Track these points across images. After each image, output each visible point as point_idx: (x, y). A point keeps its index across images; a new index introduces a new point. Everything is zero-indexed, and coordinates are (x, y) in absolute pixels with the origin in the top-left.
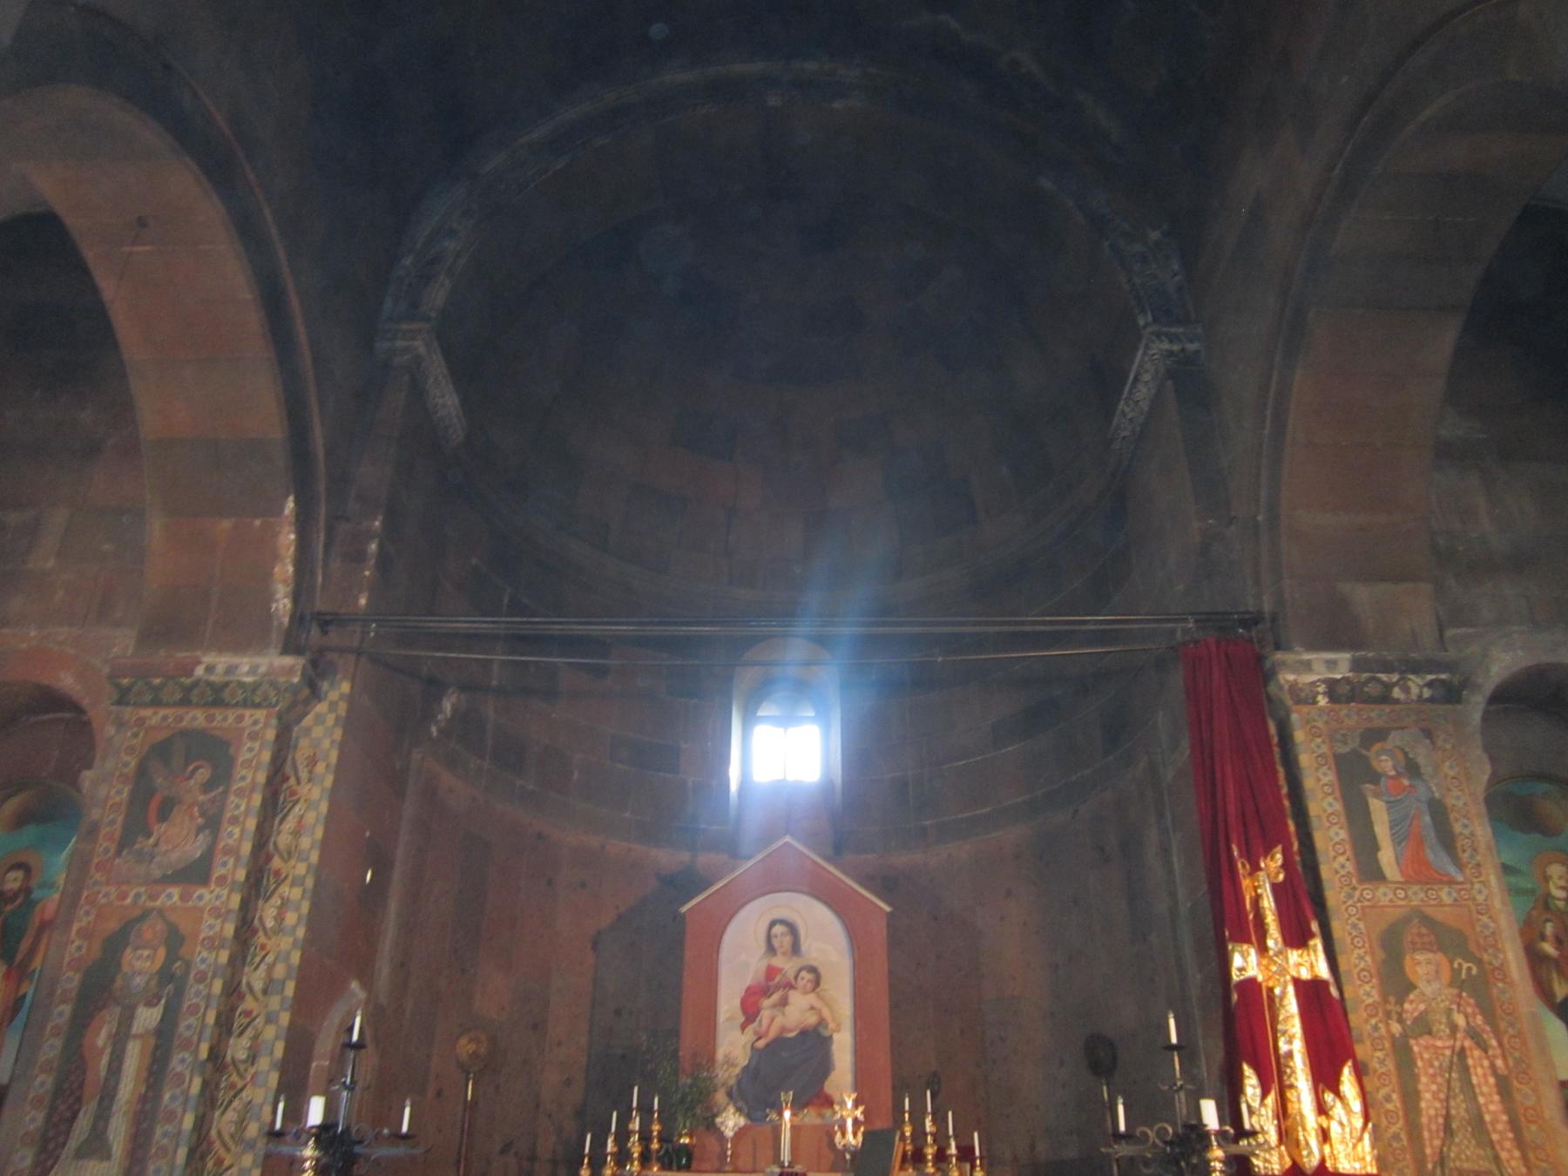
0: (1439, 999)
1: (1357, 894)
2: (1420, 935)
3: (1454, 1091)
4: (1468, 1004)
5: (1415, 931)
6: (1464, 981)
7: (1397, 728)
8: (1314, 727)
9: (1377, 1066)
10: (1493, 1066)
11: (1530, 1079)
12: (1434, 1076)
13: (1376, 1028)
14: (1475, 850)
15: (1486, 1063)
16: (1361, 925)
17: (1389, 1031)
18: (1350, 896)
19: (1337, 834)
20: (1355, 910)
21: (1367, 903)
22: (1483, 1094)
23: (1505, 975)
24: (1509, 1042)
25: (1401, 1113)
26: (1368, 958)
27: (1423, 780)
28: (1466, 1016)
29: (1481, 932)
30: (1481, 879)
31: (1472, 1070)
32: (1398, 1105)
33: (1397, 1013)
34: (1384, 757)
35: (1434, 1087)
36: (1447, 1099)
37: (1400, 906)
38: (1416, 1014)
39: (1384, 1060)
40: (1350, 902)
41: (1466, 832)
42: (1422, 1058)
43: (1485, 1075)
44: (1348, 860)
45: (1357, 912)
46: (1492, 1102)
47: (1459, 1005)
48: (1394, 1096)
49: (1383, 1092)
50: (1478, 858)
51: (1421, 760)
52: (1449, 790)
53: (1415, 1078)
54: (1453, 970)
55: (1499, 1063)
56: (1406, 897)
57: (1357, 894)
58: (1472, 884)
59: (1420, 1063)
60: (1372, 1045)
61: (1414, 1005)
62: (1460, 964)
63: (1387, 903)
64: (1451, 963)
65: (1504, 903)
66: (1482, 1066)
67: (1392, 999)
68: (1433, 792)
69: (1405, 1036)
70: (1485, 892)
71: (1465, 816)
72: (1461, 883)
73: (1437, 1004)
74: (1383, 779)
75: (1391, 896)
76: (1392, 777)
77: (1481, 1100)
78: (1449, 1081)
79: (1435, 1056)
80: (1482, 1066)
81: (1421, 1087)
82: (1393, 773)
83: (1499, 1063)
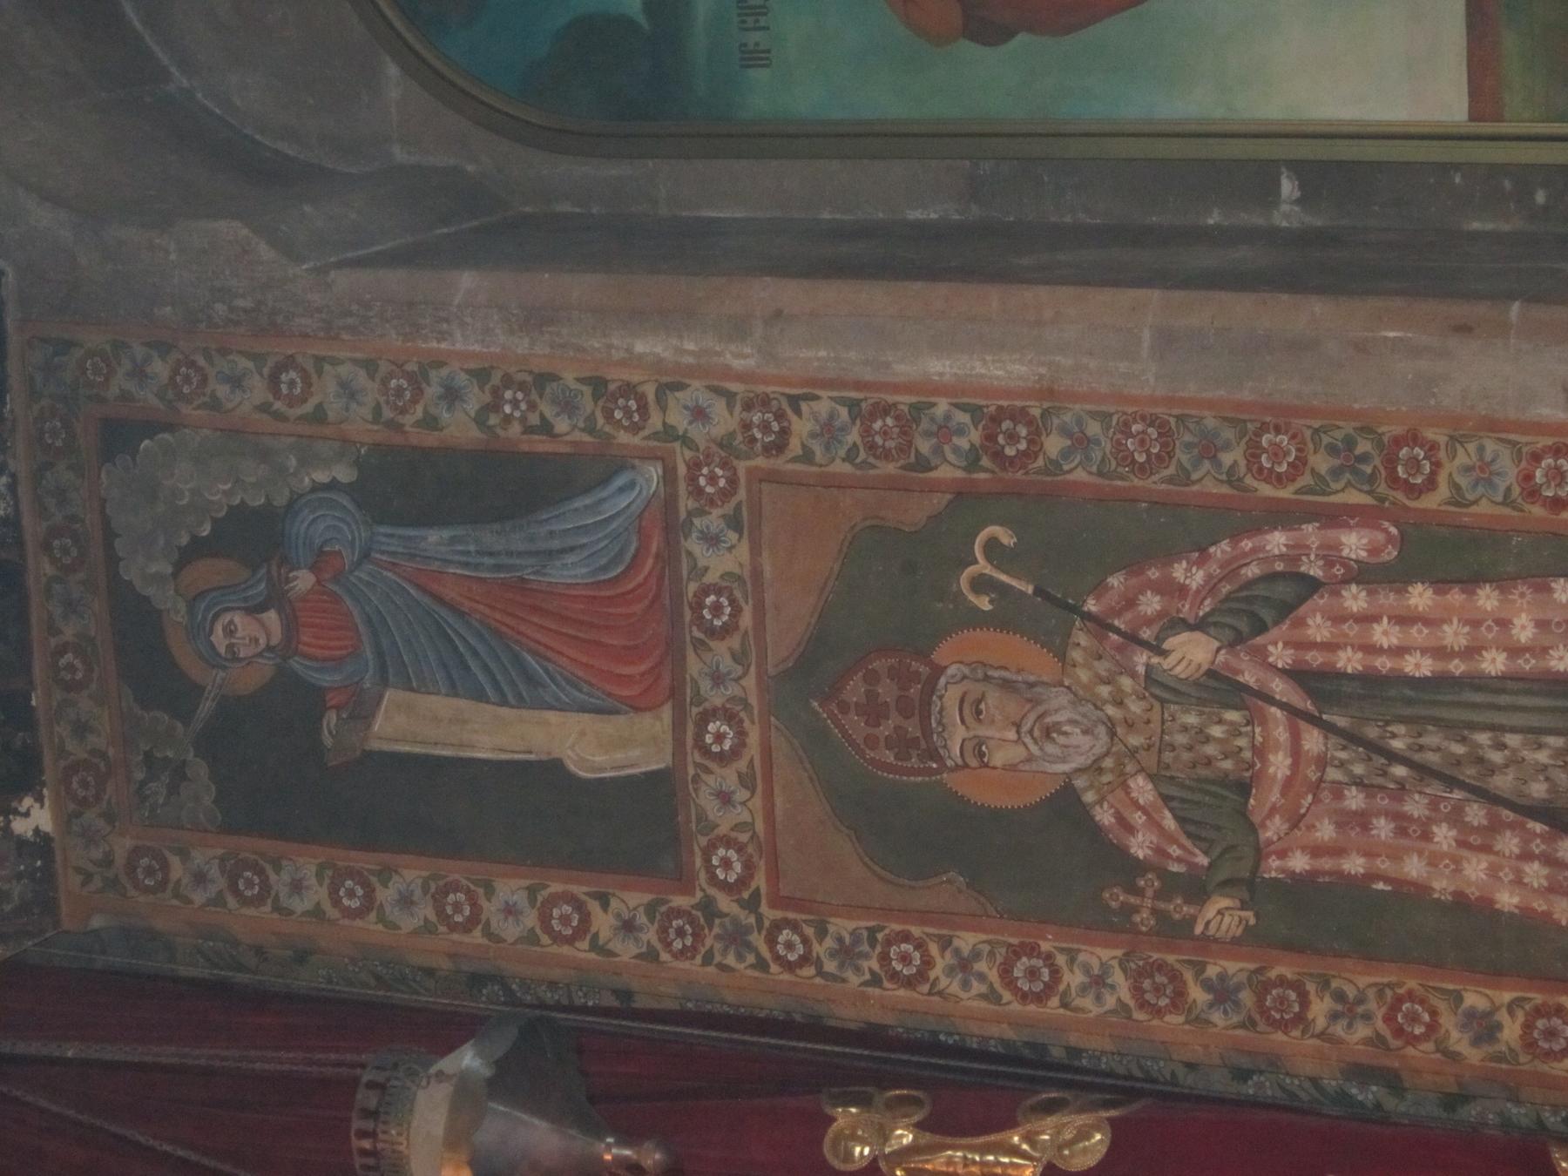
0: (1111, 710)
1: (725, 903)
2: (873, 712)
3: (1458, 762)
4: (1131, 603)
5: (856, 725)
6: (1038, 591)
7: (112, 560)
8: (131, 868)
9: (1362, 1031)
10: (1364, 574)
11: (1414, 439)
12: (1402, 823)
13: (1223, 993)
14: (543, 379)
15: (1355, 599)
16: (842, 926)
17: (1233, 946)
18: (737, 938)
19: (510, 911)
20: (785, 935)
21: (760, 881)
22: (1472, 652)
23: (1020, 415)
24: (1280, 480)
25: (1538, 998)
26: (966, 941)
27: (291, 507)
28: (1178, 624)
29: (850, 457)
30: (650, 391)
31: (1384, 664)
32: (1507, 997)
33: (1162, 895)
34: (219, 638)
35: (1444, 835)
36: (1492, 799)
37: (767, 751)
38: (1169, 822)
39: (1340, 996)
40: (758, 940)
41: (475, 400)
42: (1338, 851)
43: (1404, 620)
44: (604, 900)
45: (795, 926)
46: (1504, 624)
47: (1133, 638)
48: (1474, 999)
49: (1459, 1040)
50: (569, 377)
51: (221, 494)
52: (319, 416)
53: (1411, 894)
54: (998, 621)
55: (1354, 543)
56: (730, 718)
57: (725, 903)
58: (669, 433)
59: (1355, 865)
60: (1284, 1026)
61: (1138, 818)
62: (981, 584)
63: (757, 802)
64: (977, 619)
65: (738, 329)
66: (1367, 619)
67: (1116, 897)
68: (333, 485)
69: (1251, 888)
70: (696, 392)
71: (418, 393)
72: (669, 476)
73: (1130, 725)
74: (296, 664)
75: (728, 777)
76: (291, 627)
77: (1494, 663)
78: (1424, 771)
79: (1326, 796)
80: (1367, 619)
81: (1442, 886)
82: (272, 617)
83: (1354, 543)
